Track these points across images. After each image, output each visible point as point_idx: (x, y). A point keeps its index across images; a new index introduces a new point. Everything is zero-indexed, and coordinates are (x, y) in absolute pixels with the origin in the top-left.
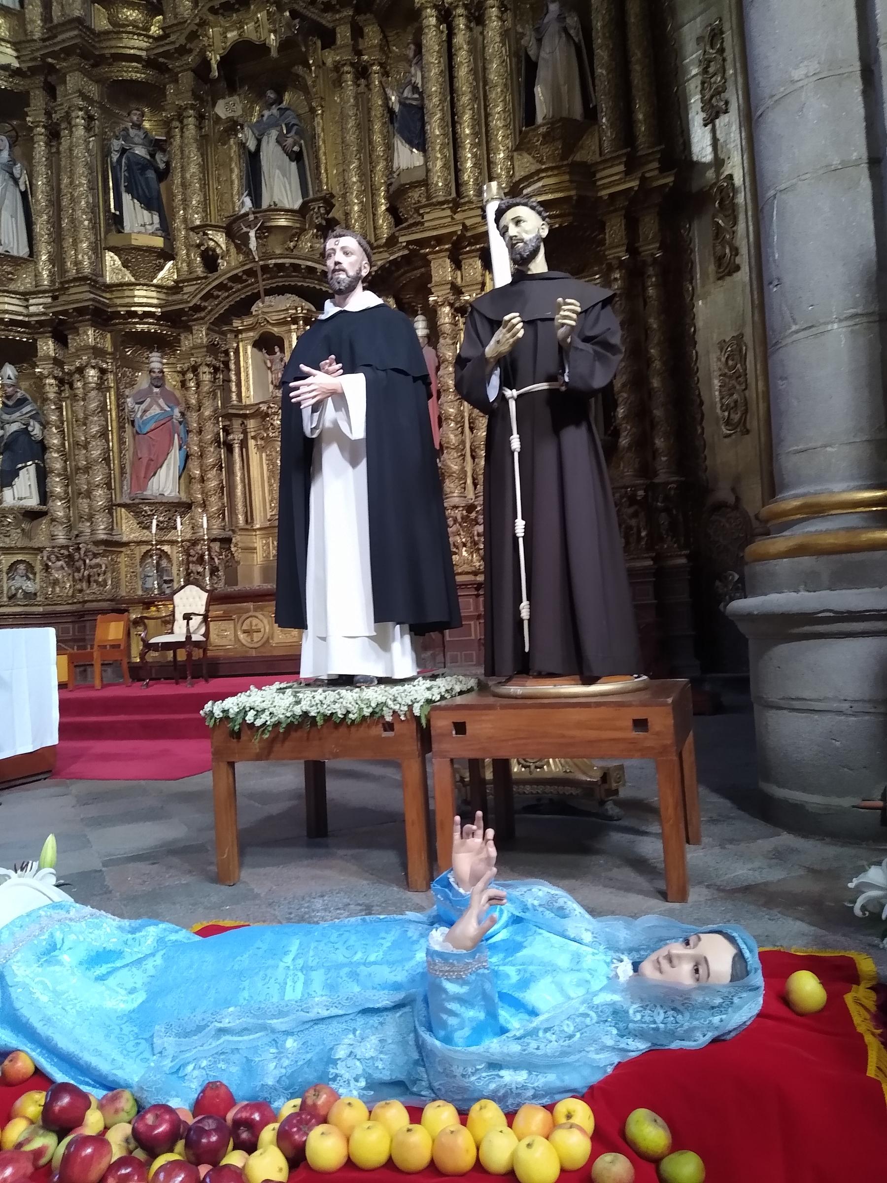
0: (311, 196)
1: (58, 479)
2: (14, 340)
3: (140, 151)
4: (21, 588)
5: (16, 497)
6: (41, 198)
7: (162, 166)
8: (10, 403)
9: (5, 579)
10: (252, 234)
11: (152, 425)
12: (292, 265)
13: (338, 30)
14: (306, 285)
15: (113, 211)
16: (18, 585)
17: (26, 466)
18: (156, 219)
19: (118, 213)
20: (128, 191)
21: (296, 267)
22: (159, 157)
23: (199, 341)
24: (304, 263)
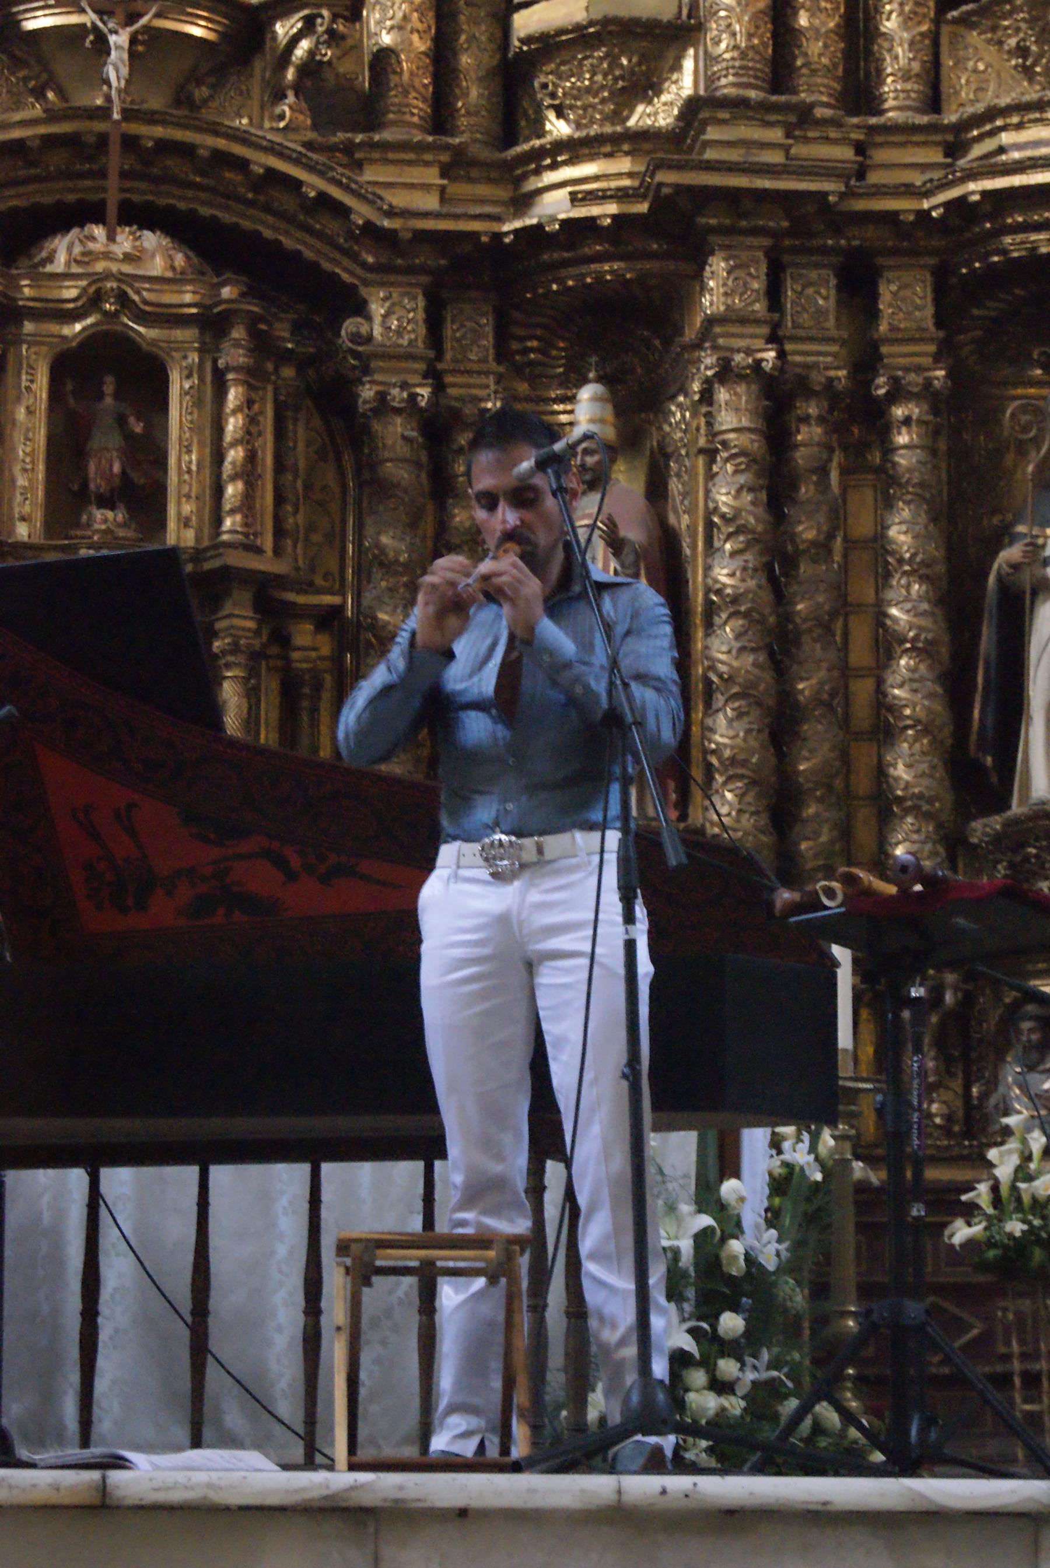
10: (119, 40)
24: (262, 161)
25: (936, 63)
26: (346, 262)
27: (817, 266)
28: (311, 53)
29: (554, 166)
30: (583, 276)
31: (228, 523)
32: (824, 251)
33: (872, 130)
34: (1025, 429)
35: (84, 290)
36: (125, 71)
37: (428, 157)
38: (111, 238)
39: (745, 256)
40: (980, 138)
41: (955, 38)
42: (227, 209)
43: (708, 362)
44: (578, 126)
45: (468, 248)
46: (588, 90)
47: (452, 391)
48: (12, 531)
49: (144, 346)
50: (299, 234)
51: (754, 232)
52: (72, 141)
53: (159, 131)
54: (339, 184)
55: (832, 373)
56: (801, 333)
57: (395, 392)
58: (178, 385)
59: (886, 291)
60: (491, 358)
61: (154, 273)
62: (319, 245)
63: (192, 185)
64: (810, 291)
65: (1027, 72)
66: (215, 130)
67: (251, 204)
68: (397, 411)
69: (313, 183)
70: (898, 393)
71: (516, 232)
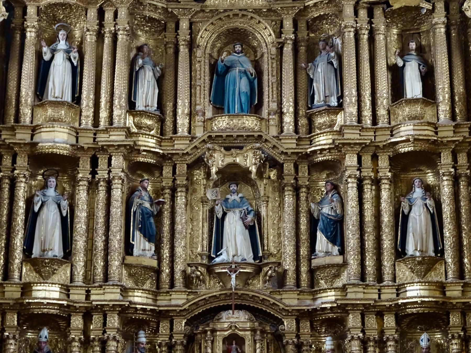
0: (260, 254)
3: (147, 205)
10: (233, 276)
13: (285, 165)
14: (256, 306)
18: (153, 248)
20: (140, 230)
24: (262, 297)
25: (395, 270)
26: (279, 314)
27: (371, 314)
28: (271, 274)
29: (320, 293)
30: (326, 316)
32: (372, 311)
33: (381, 286)
34: (413, 348)
36: (235, 282)
37: (295, 292)
38: (233, 314)
39: (356, 314)
40: (402, 288)
41: (398, 265)
42: (256, 305)
43: (349, 336)
44: (326, 283)
45: (302, 311)
46: (326, 276)
47: (301, 338)
50: (270, 309)
51: (357, 310)
53: (242, 292)
55: (375, 336)
56: (368, 328)
57: (290, 340)
58: (247, 343)
59: (385, 318)
60: (309, 331)
61: (241, 321)
62: (274, 311)
64: (370, 319)
65: (413, 272)
66: (252, 291)
67: (261, 304)
68: (291, 344)
69: (272, 301)
70: (388, 339)
71: (312, 309)
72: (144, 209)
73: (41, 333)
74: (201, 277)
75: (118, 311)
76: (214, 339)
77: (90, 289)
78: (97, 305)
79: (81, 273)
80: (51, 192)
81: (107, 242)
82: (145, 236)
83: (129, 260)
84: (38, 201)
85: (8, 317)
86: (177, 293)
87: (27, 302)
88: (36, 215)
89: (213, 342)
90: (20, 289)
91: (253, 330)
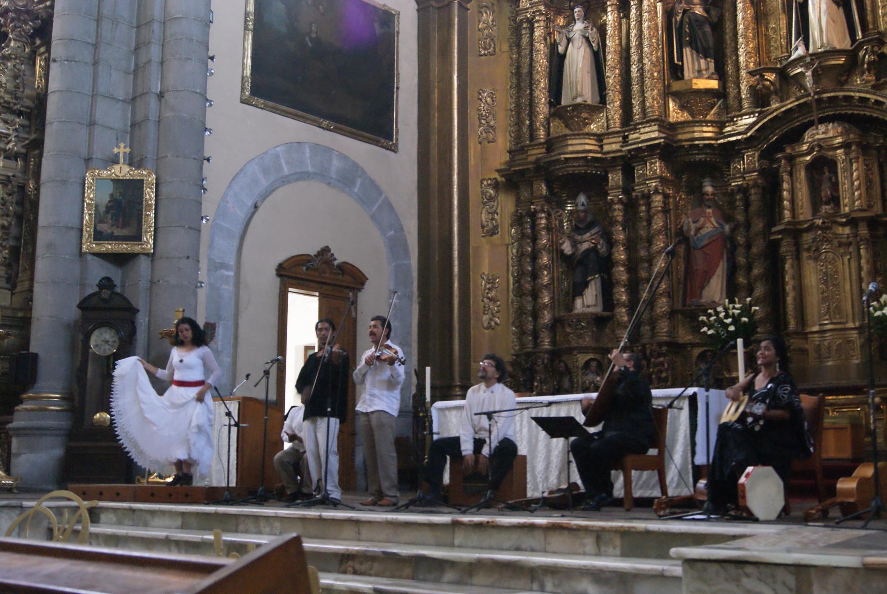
1: (623, 290)
2: (591, 173)
3: (699, 10)
4: (593, 382)
5: (585, 304)
6: (611, 58)
7: (715, 19)
8: (581, 226)
9: (580, 375)
10: (809, 73)
11: (705, 242)
12: (845, 97)
15: (676, 62)
16: (591, 380)
17: (594, 278)
18: (712, 65)
19: (680, 63)
21: (846, 98)
22: (713, 13)
23: (752, 166)
31: (857, 203)
35: (809, 146)
36: (811, 82)
48: (798, 218)
49: (830, 158)
52: (805, 103)
54: (879, 96)
58: (840, 166)
63: (843, 106)
67: (860, 107)
69: (873, 98)
72: (693, 17)
73: (577, 201)
74: (772, 88)
75: (658, 154)
76: (792, 169)
77: (626, 134)
78: (629, 151)
79: (617, 117)
80: (579, 26)
81: (641, 70)
82: (698, 52)
83: (676, 86)
84: (561, 40)
85: (535, 186)
86: (744, 117)
87: (544, 163)
88: (563, 57)
89: (791, 174)
90: (544, 150)
91: (846, 146)
